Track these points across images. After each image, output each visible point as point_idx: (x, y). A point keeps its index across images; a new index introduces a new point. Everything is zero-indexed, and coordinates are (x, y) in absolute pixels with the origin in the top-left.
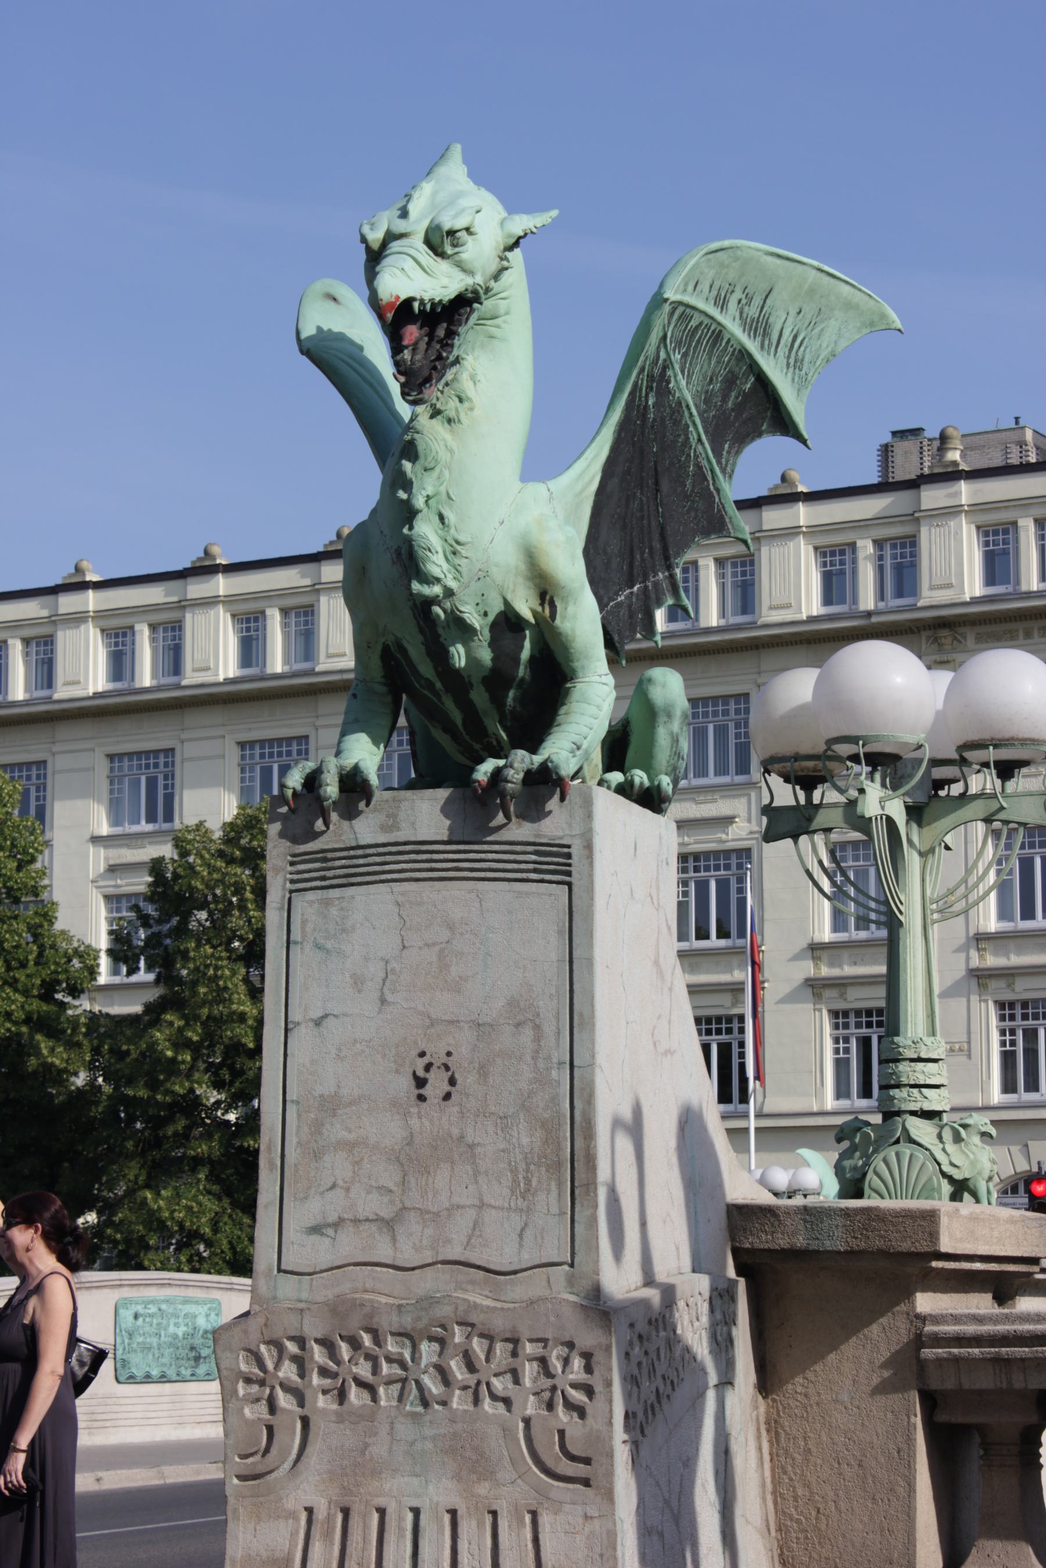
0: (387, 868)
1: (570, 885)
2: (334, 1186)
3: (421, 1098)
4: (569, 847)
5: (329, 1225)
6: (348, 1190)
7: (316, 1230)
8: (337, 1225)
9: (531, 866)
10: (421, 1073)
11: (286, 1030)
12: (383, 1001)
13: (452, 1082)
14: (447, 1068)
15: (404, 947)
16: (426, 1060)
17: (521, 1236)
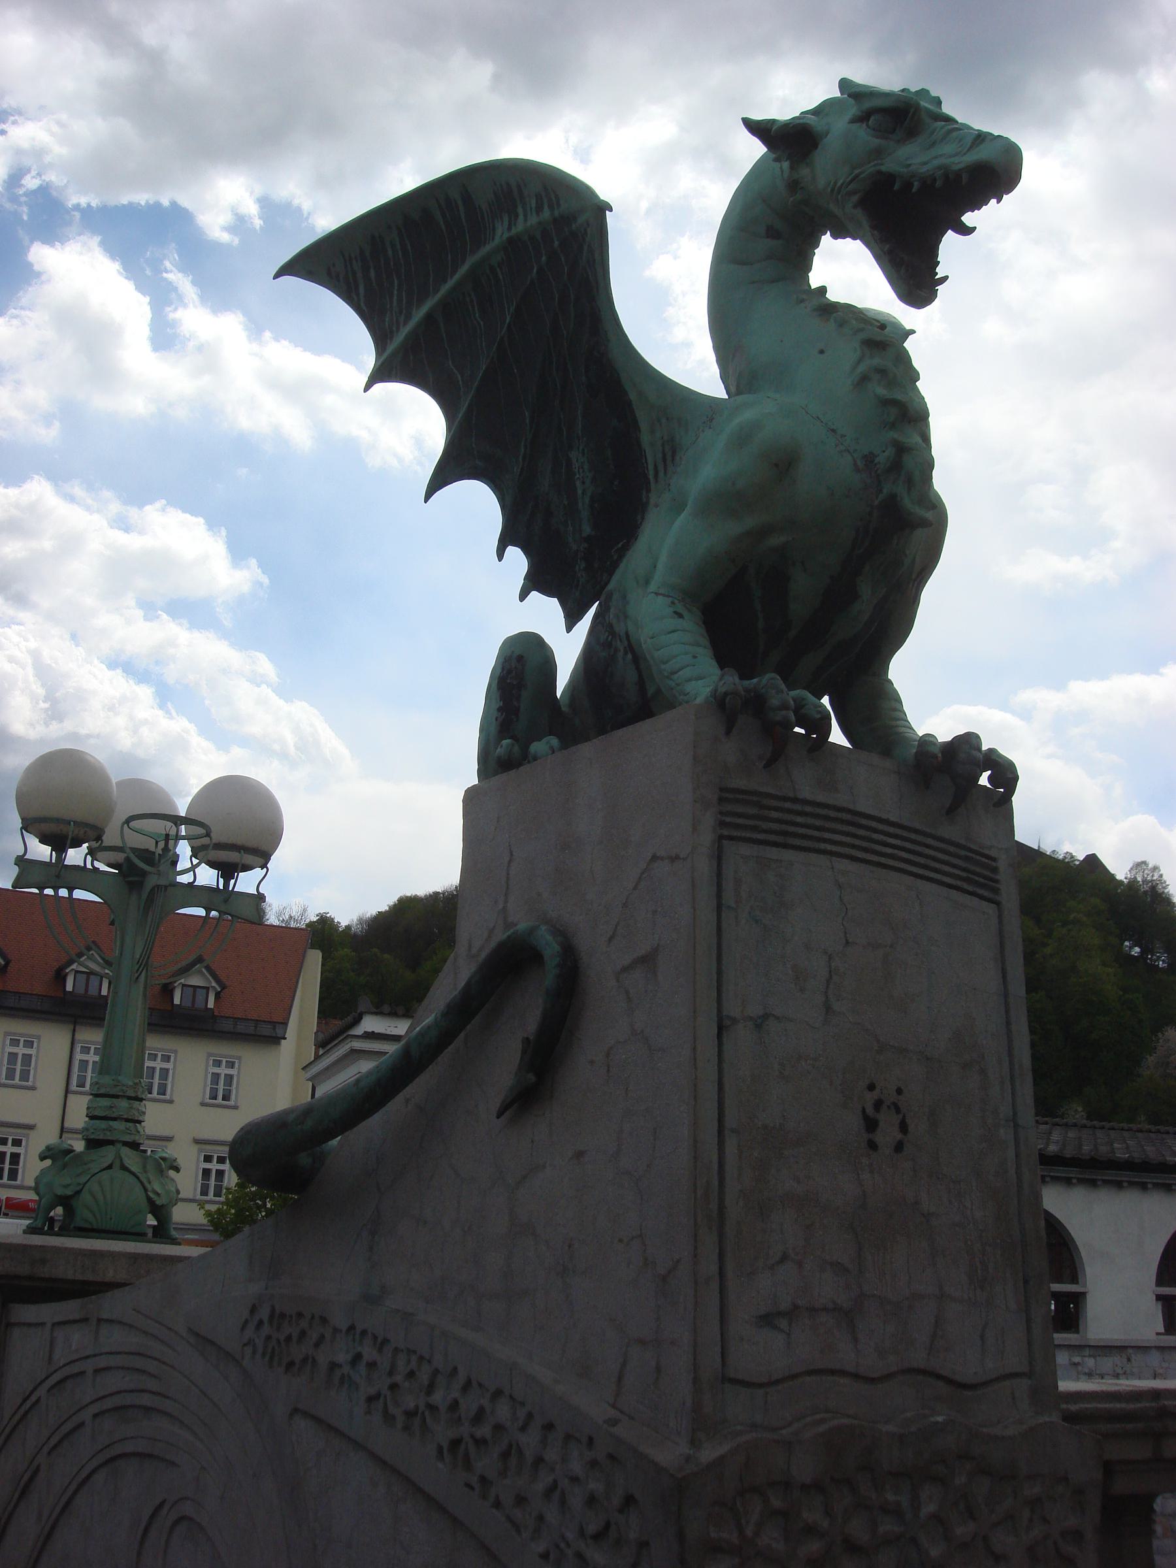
0: (875, 836)
1: (998, 904)
2: (784, 1258)
3: (872, 1145)
4: (994, 859)
5: (780, 1314)
6: (800, 1264)
7: (767, 1320)
8: (792, 1313)
9: (964, 874)
10: (870, 1111)
11: (721, 1029)
12: (828, 1009)
13: (904, 1127)
14: (898, 1110)
15: (847, 942)
16: (876, 1094)
17: (982, 1337)
